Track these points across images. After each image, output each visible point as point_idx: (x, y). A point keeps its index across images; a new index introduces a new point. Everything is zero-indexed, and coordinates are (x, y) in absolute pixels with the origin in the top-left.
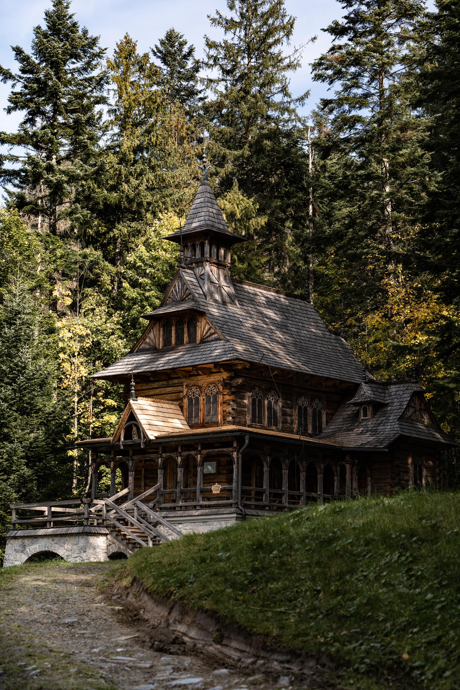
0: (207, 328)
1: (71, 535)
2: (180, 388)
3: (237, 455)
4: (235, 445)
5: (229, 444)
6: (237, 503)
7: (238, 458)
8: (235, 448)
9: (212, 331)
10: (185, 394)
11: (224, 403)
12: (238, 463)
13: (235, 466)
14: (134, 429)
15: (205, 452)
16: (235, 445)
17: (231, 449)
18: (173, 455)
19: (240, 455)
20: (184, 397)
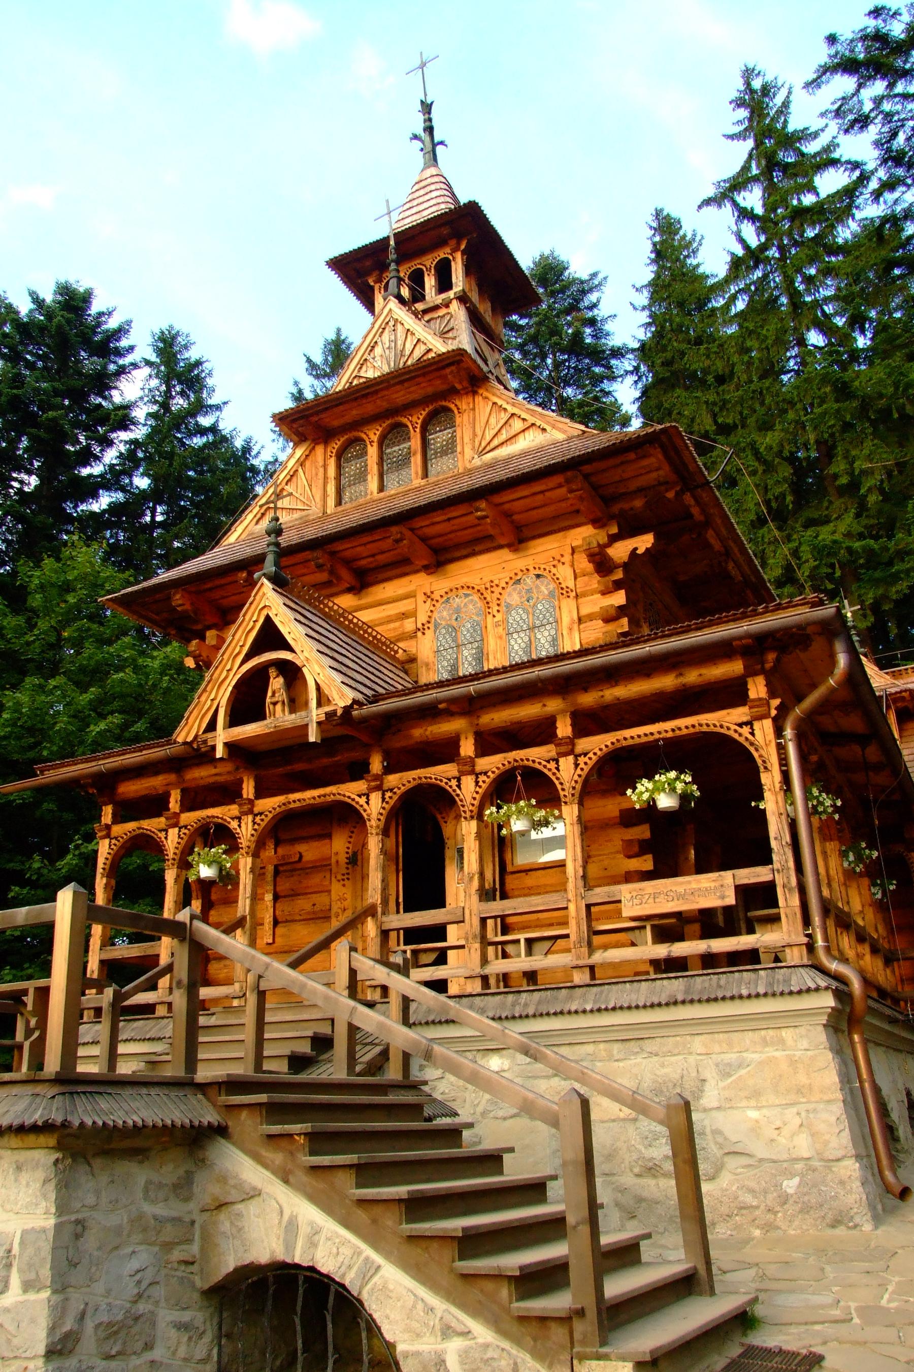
3: (779, 732)
4: (757, 688)
5: (731, 694)
6: (811, 947)
9: (517, 425)
10: (422, 618)
12: (783, 761)
13: (770, 779)
14: (277, 683)
15: (597, 744)
16: (757, 688)
19: (789, 733)
20: (423, 629)
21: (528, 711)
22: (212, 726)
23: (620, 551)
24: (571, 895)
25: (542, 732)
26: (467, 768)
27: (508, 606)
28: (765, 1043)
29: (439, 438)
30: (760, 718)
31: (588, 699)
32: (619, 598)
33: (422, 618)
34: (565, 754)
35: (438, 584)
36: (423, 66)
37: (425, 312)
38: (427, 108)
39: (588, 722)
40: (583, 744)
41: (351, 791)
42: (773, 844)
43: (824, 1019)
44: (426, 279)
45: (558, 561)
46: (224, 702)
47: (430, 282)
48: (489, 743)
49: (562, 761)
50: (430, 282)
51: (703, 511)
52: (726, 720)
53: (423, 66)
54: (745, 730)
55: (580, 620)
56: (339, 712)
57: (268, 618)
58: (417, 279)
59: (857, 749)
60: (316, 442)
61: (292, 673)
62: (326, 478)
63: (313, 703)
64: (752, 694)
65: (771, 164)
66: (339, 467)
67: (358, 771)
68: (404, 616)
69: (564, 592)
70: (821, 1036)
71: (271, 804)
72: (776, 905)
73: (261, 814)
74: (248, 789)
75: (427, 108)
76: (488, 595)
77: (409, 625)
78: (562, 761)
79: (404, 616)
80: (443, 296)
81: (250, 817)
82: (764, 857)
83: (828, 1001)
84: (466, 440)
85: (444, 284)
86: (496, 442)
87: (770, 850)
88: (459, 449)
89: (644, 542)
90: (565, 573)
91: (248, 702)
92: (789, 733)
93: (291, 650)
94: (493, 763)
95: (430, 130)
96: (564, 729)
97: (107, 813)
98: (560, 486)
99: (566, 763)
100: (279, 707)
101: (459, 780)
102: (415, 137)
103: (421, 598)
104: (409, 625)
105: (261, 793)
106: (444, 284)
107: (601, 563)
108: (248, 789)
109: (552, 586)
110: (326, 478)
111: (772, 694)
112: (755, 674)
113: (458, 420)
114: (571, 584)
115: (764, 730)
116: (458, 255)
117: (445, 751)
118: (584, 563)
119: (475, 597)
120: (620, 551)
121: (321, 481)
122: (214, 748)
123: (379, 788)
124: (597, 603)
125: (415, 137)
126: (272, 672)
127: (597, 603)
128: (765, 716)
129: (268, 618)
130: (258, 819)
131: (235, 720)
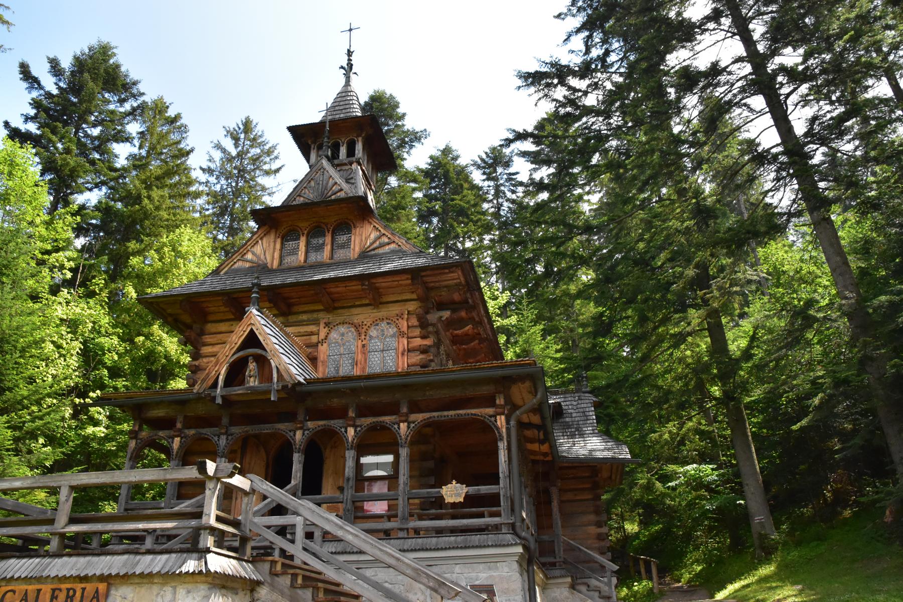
0: (373, 236)
1: (147, 578)
2: (313, 328)
3: (508, 422)
4: (500, 401)
5: (490, 401)
7: (508, 429)
8: (501, 406)
9: (386, 240)
10: (322, 335)
11: (409, 351)
13: (502, 446)
14: (252, 366)
15: (419, 417)
17: (490, 411)
18: (336, 424)
19: (512, 423)
20: (322, 342)
21: (386, 398)
22: (215, 385)
24: (400, 493)
26: (351, 423)
27: (371, 337)
28: (490, 569)
29: (342, 239)
30: (501, 414)
33: (322, 335)
34: (403, 422)
36: (350, 30)
37: (338, 165)
38: (350, 53)
39: (415, 408)
40: (413, 417)
42: (501, 475)
43: (517, 558)
44: (341, 148)
45: (400, 316)
46: (223, 371)
47: (343, 151)
49: (401, 424)
50: (343, 151)
51: (474, 302)
53: (350, 30)
54: (493, 419)
55: (409, 351)
56: (290, 386)
57: (252, 330)
58: (336, 148)
59: (536, 432)
60: (271, 228)
61: (263, 361)
62: (274, 249)
63: (275, 380)
64: (498, 402)
66: (282, 244)
67: (290, 417)
68: (312, 334)
69: (401, 334)
70: (515, 566)
72: (500, 506)
73: (232, 435)
74: (225, 421)
75: (350, 53)
76: (360, 329)
77: (314, 339)
78: (401, 424)
79: (312, 334)
80: (351, 159)
81: (225, 437)
82: (495, 480)
83: (520, 550)
84: (357, 242)
85: (351, 152)
86: (372, 248)
87: (499, 478)
88: (352, 246)
90: (404, 325)
91: (236, 372)
92: (512, 423)
93: (265, 350)
95: (350, 66)
98: (407, 279)
99: (403, 426)
100: (252, 379)
101: (346, 429)
102: (342, 67)
103: (322, 325)
104: (314, 339)
105: (232, 423)
106: (351, 152)
107: (423, 324)
108: (225, 421)
109: (395, 329)
110: (274, 249)
111: (506, 403)
112: (500, 393)
113: (353, 231)
114: (405, 329)
115: (501, 421)
116: (360, 139)
118: (414, 321)
119: (353, 330)
120: (433, 317)
121: (272, 251)
122: (214, 398)
123: (301, 428)
125: (342, 67)
126: (250, 358)
127: (418, 342)
128: (502, 414)
129: (252, 330)
130: (230, 438)
131: (228, 382)
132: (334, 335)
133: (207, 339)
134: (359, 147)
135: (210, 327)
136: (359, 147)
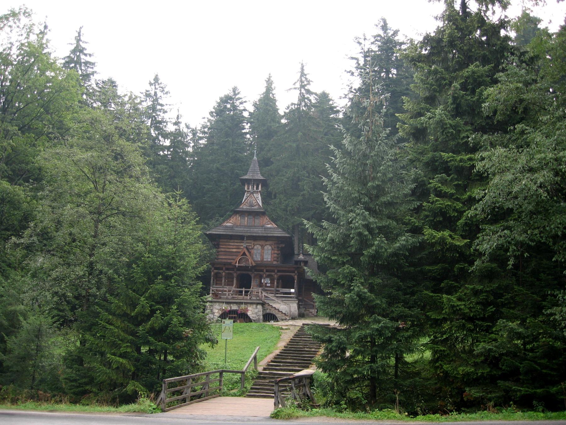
4: (296, 272)
15: (279, 274)
16: (296, 272)
17: (294, 274)
21: (272, 269)
23: (280, 246)
25: (273, 271)
31: (279, 269)
32: (279, 252)
35: (256, 243)
39: (279, 271)
41: (250, 273)
47: (255, 187)
48: (267, 271)
50: (255, 187)
52: (293, 274)
65: (302, 86)
71: (239, 272)
85: (257, 188)
89: (283, 245)
94: (268, 273)
96: (276, 271)
97: (213, 269)
106: (257, 188)
107: (278, 247)
115: (296, 277)
117: (262, 271)
120: (280, 246)
124: (276, 252)
127: (276, 252)
132: (255, 247)
133: (221, 243)
134: (260, 187)
135: (221, 240)
136: (260, 187)
